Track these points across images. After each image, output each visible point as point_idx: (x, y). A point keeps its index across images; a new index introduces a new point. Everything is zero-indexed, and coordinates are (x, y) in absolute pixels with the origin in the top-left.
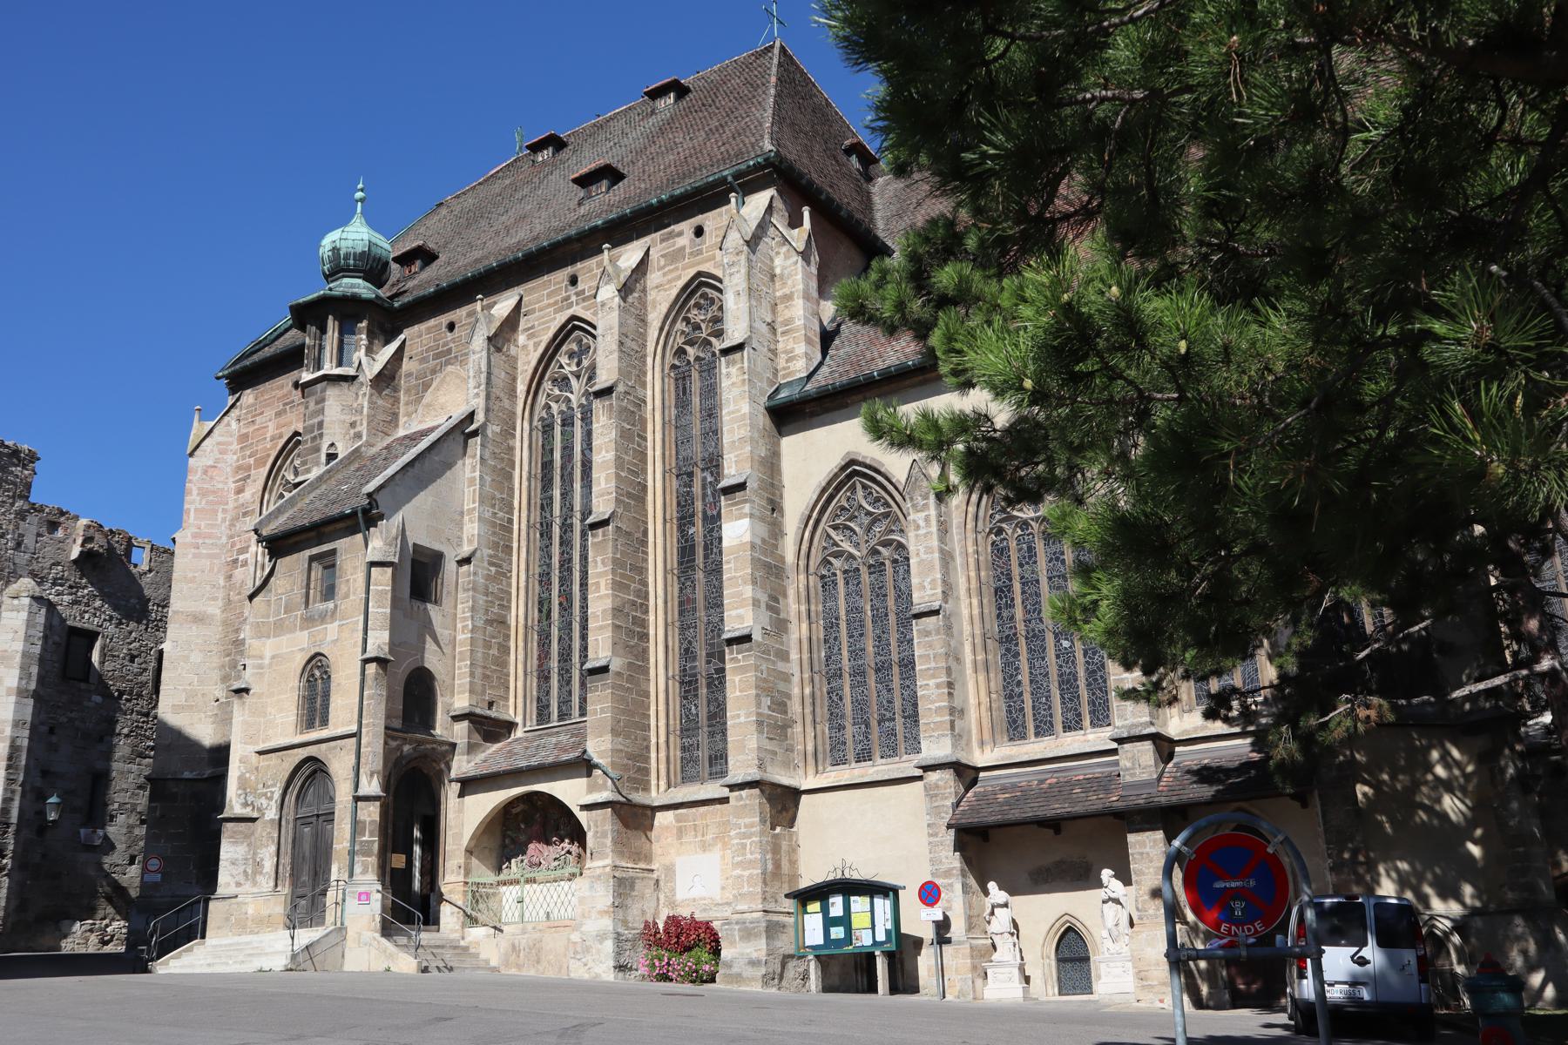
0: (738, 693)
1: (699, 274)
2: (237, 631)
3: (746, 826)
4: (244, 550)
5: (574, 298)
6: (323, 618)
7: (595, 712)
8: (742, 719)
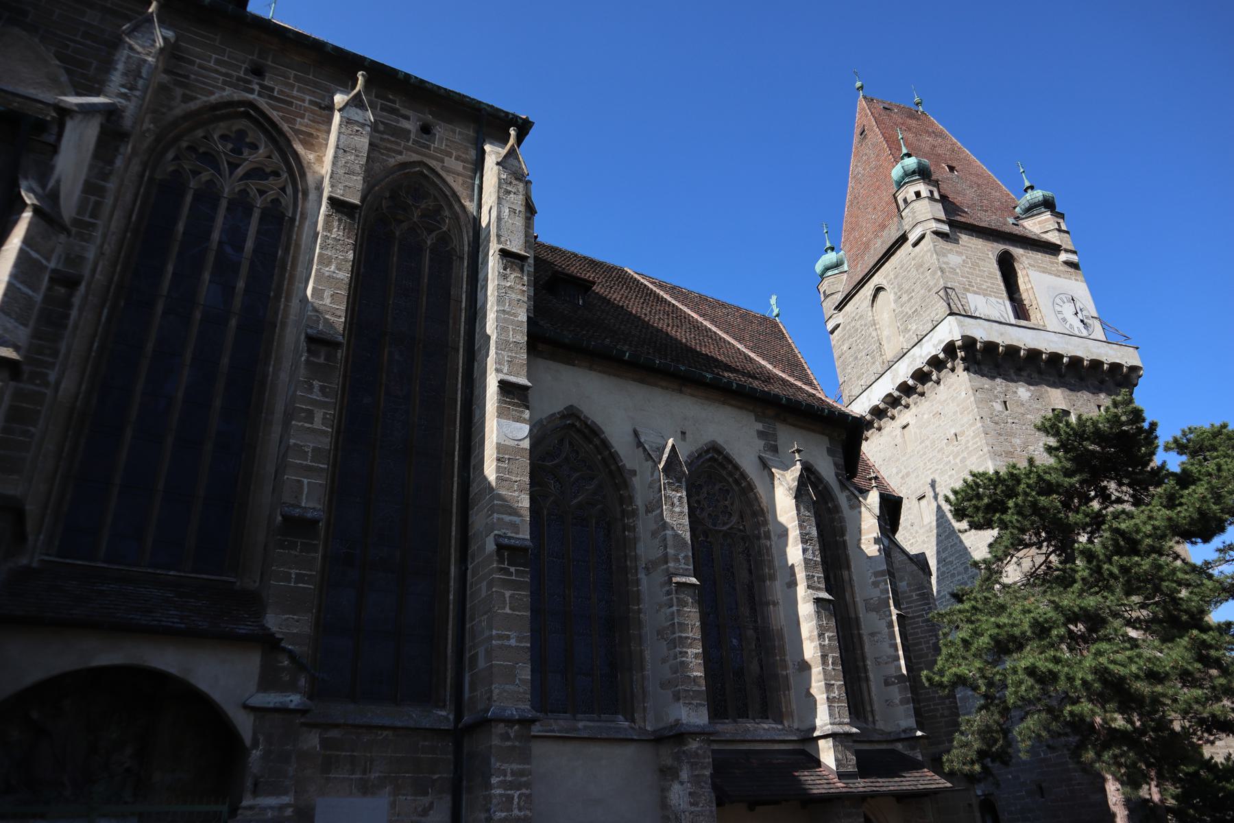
0: (508, 610)
1: (421, 163)
3: (513, 773)
5: (257, 87)
7: (287, 577)
8: (513, 642)
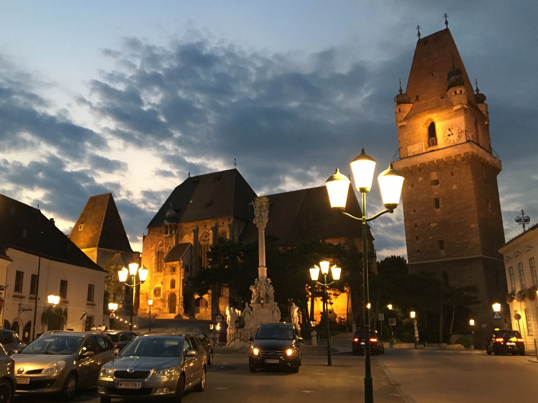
2: (152, 269)
4: (153, 257)
6: (174, 274)
